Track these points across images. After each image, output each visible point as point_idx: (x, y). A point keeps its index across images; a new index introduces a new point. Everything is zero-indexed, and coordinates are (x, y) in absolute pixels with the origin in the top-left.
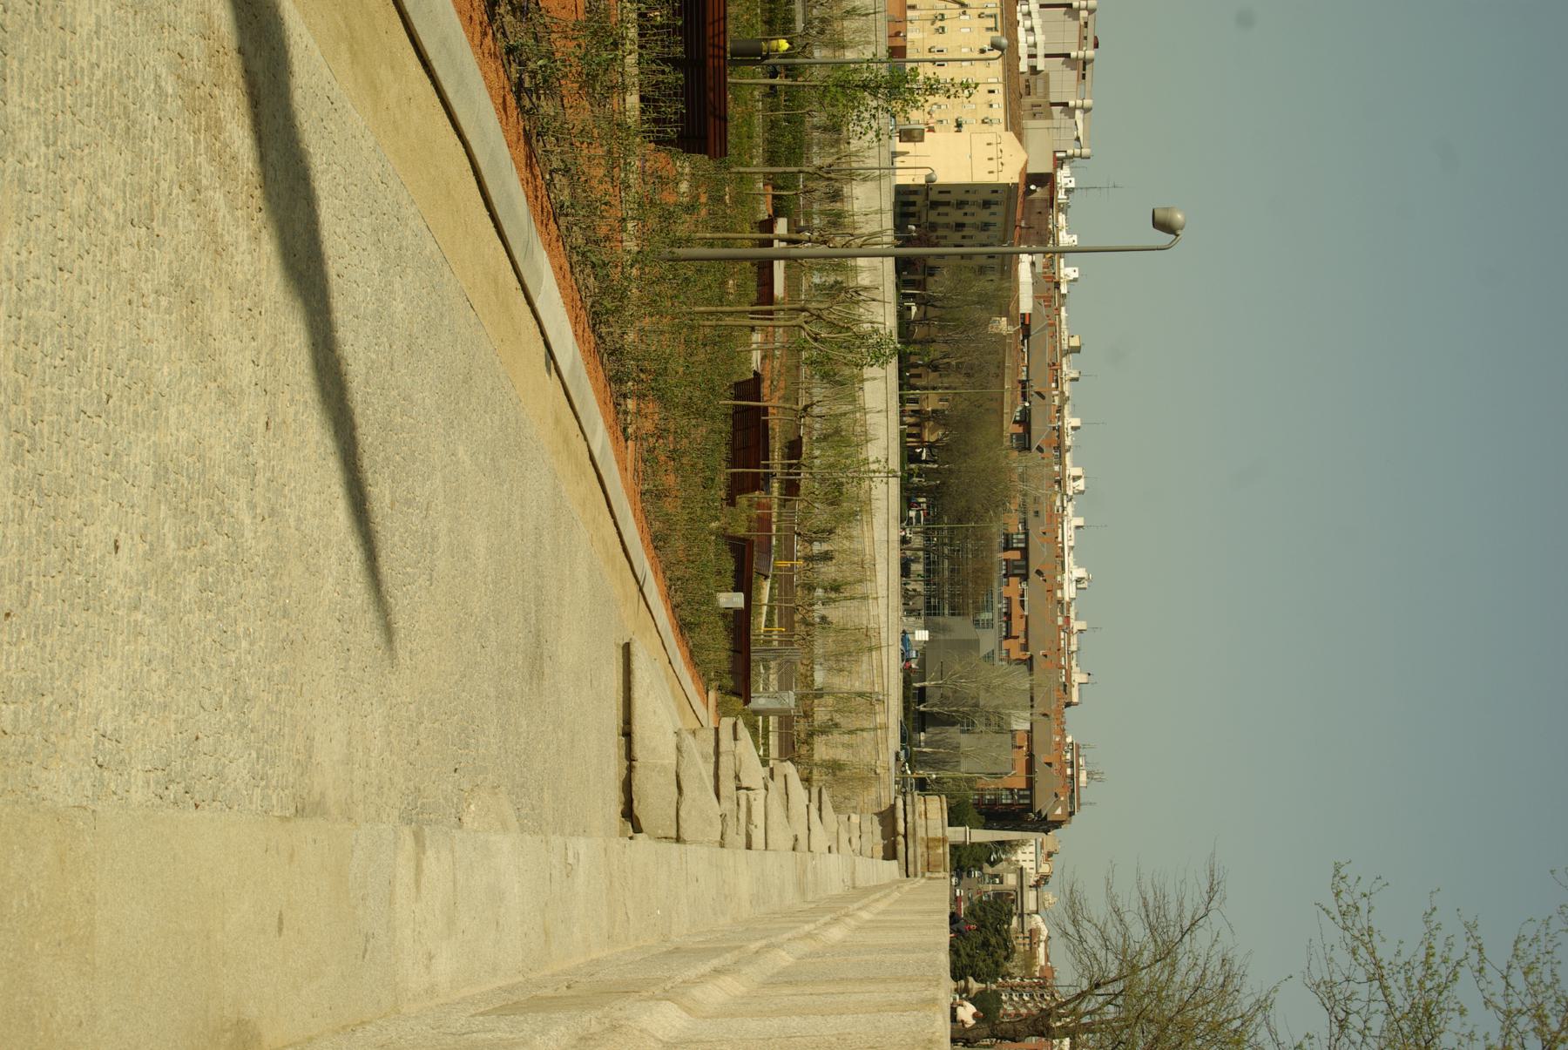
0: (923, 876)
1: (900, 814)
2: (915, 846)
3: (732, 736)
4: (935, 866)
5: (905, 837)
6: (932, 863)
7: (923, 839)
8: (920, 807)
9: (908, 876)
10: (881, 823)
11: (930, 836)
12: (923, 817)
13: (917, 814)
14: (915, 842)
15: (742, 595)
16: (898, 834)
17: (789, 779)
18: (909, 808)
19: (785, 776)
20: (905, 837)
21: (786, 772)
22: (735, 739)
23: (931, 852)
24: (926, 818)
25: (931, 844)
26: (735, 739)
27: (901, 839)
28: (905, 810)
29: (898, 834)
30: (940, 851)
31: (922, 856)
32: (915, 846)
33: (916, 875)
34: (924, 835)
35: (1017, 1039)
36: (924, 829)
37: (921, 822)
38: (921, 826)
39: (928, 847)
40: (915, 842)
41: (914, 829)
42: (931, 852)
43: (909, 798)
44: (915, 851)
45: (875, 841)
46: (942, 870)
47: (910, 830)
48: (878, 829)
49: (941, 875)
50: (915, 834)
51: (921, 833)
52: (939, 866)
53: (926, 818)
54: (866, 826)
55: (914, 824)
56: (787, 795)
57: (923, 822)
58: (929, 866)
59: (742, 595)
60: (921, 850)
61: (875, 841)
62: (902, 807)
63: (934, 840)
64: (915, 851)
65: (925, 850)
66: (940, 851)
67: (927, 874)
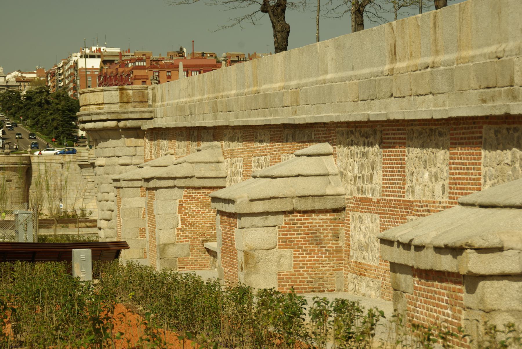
0: (150, 106)
1: (100, 125)
2: (127, 112)
3: (496, 255)
4: (143, 96)
5: (119, 120)
6: (141, 99)
7: (121, 107)
8: (93, 109)
9: (152, 118)
10: (106, 139)
11: (118, 100)
12: (101, 106)
13: (100, 111)
14: (124, 113)
15: (75, 251)
16: (117, 126)
17: (254, 197)
18: (94, 118)
19: (251, 200)
20: (119, 120)
21: (248, 200)
22: (500, 249)
23: (132, 99)
24: (102, 104)
25: (125, 100)
26: (500, 249)
27: (121, 124)
28: (95, 121)
29: (117, 126)
30: (131, 92)
31: (135, 107)
32: (128, 112)
33: (151, 112)
34: (118, 106)
35: (287, 30)
36: (113, 106)
37: (106, 108)
38: (110, 108)
39: (128, 102)
40: (124, 113)
41: (113, 113)
42: (132, 99)
43: (80, 119)
44: (132, 112)
45: (122, 145)
46: (146, 91)
47: (114, 116)
48: (112, 142)
49: (150, 92)
50: (118, 113)
51: (116, 108)
52: (143, 93)
53: (102, 104)
54: (109, 152)
55: (108, 113)
56: (270, 199)
57: (106, 106)
58: (144, 102)
59: (76, 251)
60: (130, 108)
61: (122, 145)
62: (93, 123)
63: (121, 97)
64: (132, 112)
65: (130, 105)
66: (131, 92)
67: (150, 102)
